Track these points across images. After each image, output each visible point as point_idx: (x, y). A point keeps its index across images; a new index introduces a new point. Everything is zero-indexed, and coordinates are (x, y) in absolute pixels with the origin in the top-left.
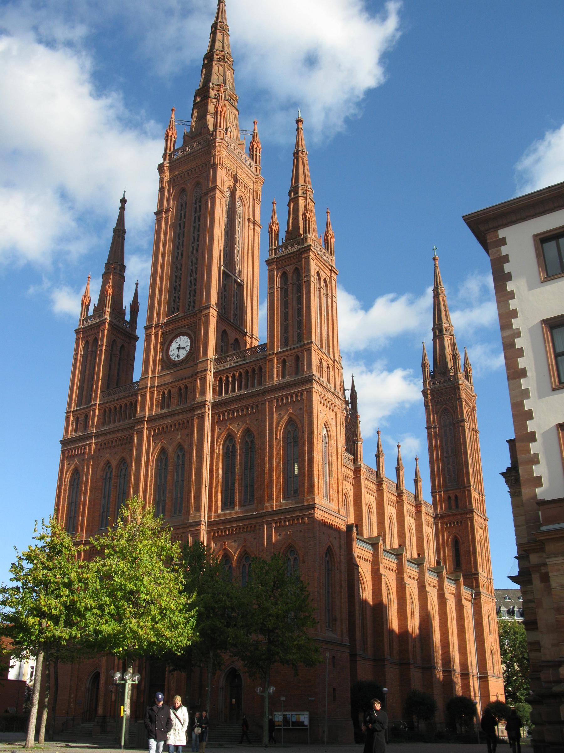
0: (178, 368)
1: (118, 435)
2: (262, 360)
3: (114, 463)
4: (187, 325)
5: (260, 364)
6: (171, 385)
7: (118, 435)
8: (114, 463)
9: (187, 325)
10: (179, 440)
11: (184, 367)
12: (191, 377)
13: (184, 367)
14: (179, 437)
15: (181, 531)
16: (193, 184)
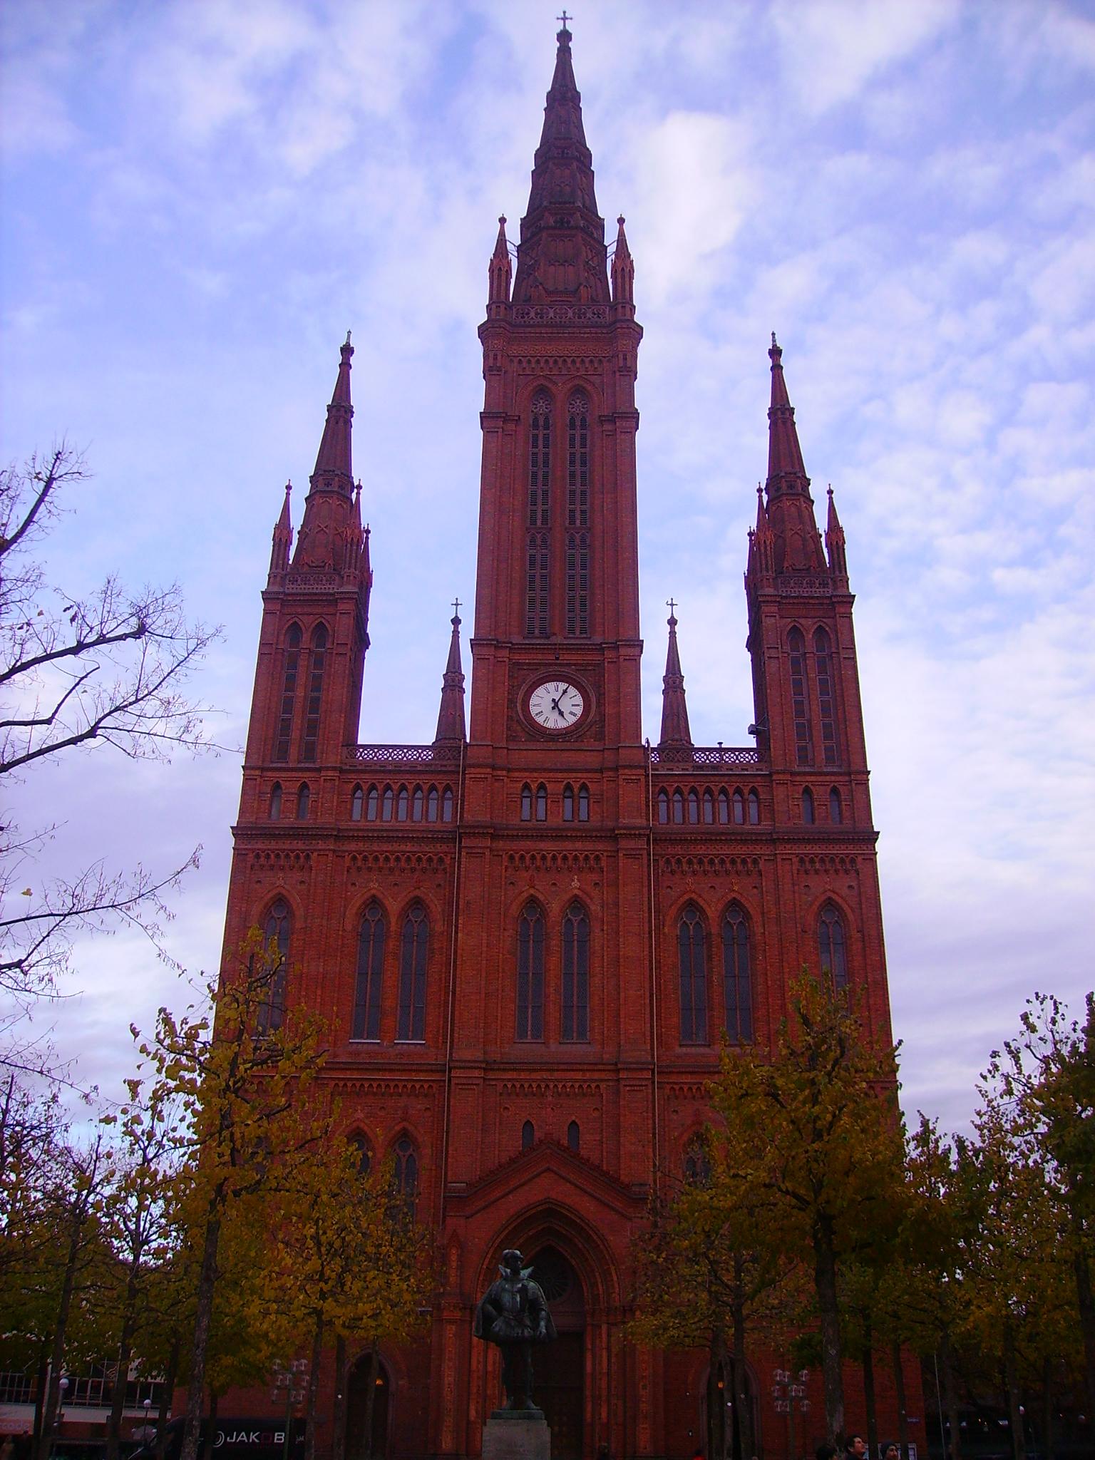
0: (559, 746)
1: (403, 847)
2: (759, 779)
3: (393, 906)
4: (575, 665)
5: (756, 785)
6: (547, 775)
7: (403, 847)
8: (393, 906)
9: (575, 665)
10: (576, 892)
11: (576, 746)
12: (595, 771)
13: (576, 746)
14: (576, 884)
15: (597, 1076)
16: (568, 386)
